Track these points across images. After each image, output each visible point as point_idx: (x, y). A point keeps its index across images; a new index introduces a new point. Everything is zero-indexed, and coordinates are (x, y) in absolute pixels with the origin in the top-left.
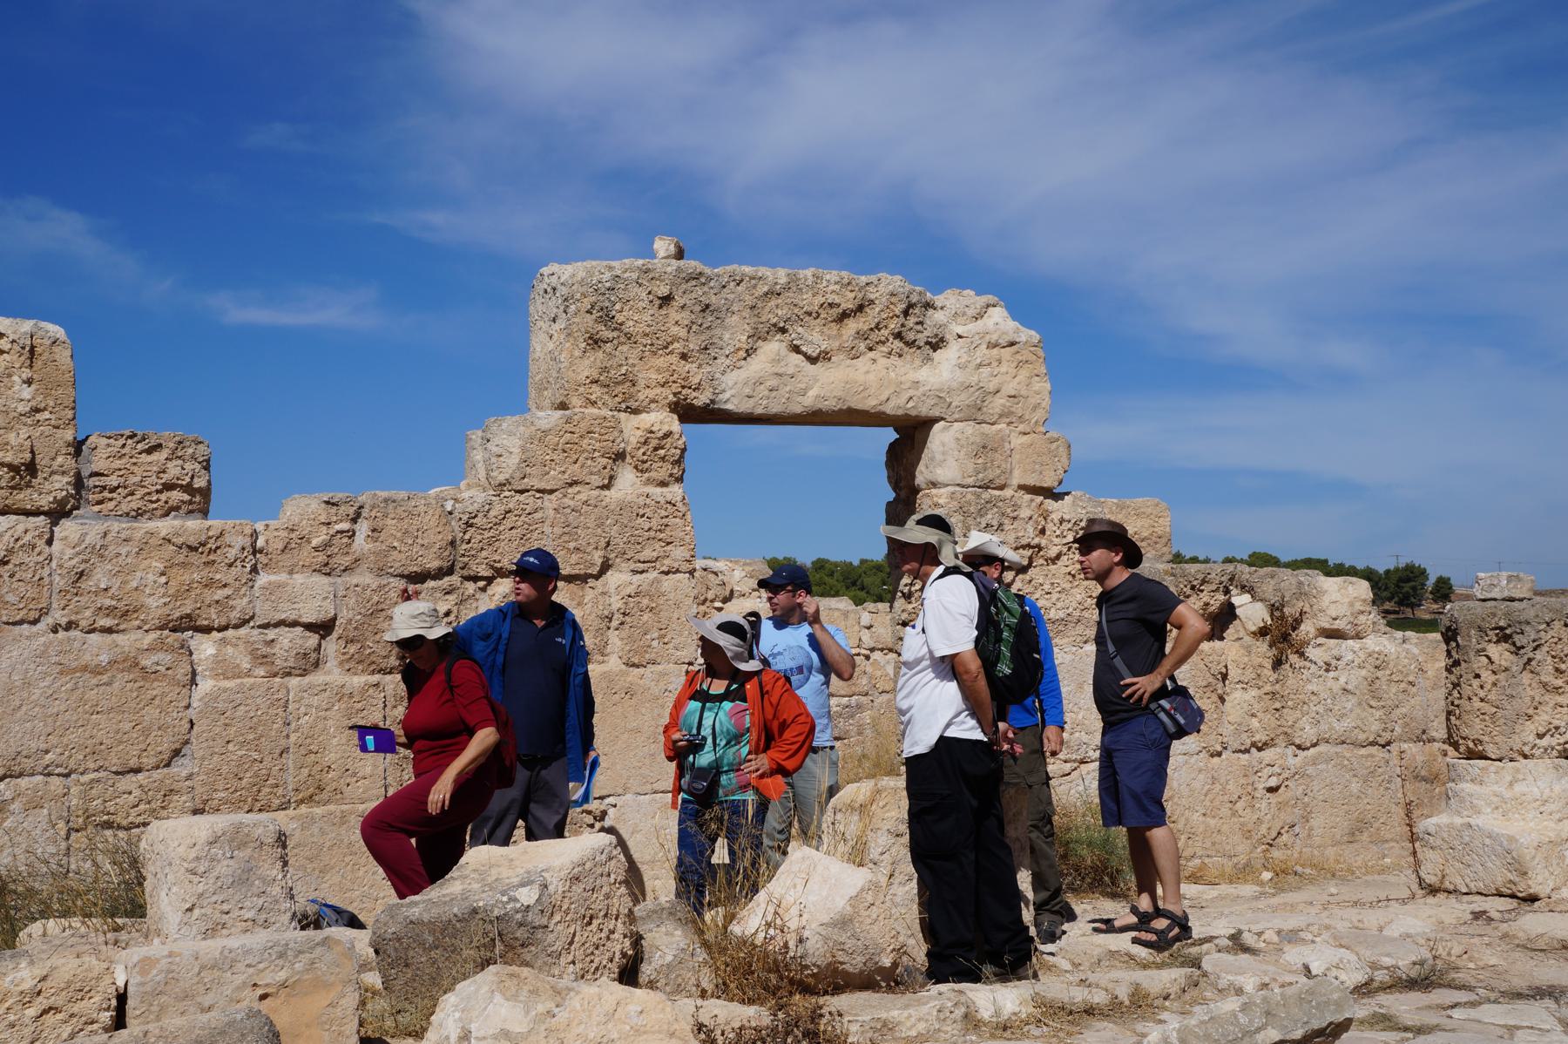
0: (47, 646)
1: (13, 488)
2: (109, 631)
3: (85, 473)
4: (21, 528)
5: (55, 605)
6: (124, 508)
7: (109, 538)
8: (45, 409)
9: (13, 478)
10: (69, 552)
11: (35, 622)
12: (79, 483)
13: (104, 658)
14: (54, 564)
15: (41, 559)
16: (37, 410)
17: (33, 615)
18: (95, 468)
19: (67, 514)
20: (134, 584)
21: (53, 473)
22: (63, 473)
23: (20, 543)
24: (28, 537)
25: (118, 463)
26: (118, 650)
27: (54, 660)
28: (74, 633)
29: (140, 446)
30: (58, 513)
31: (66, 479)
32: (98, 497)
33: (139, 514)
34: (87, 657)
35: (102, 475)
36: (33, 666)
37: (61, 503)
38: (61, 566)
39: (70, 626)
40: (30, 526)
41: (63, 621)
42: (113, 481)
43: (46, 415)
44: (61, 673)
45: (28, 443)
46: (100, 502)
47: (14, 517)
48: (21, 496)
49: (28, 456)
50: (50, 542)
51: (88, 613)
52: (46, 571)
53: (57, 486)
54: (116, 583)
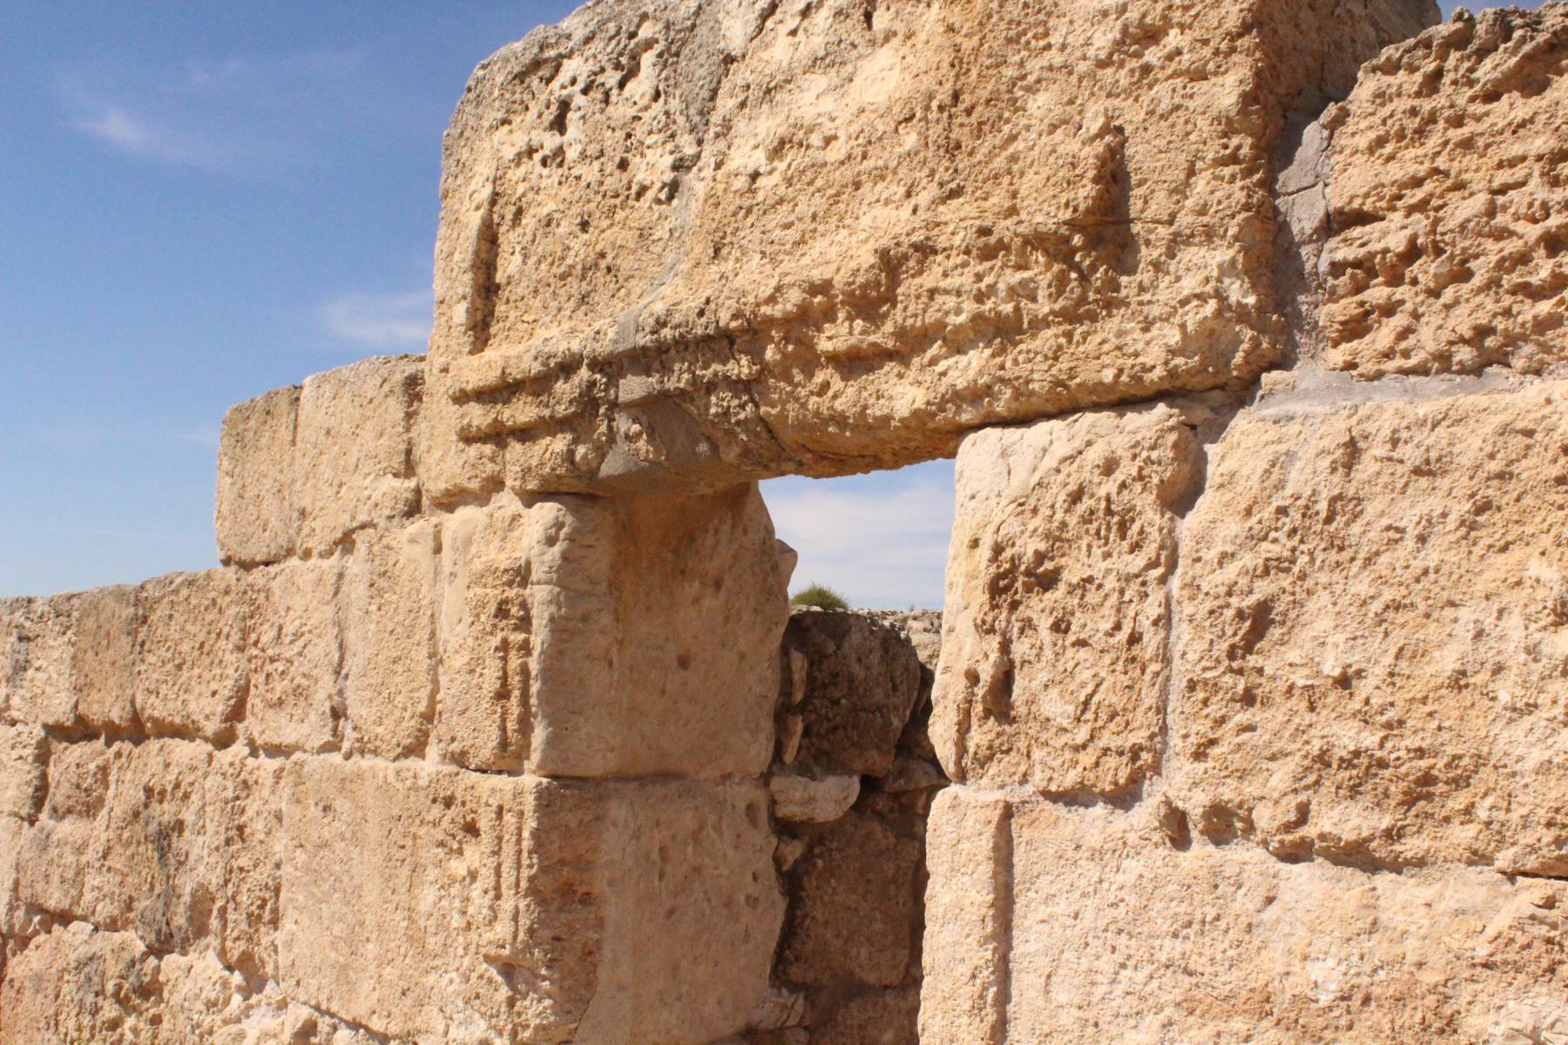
0: (1148, 888)
1: (1070, 316)
2: (1355, 856)
3: (1304, 216)
4: (1095, 455)
5: (1175, 740)
6: (1428, 339)
7: (1367, 467)
8: (1167, 23)
9: (1061, 283)
10: (1233, 527)
11: (1124, 797)
12: (1273, 259)
13: (1326, 976)
14: (1175, 582)
15: (1138, 561)
16: (1151, 36)
17: (1116, 771)
18: (1335, 197)
19: (1243, 392)
20: (1447, 661)
21: (1176, 243)
22: (1209, 234)
23: (1081, 508)
24: (1109, 487)
25: (1411, 161)
26: (1378, 947)
27: (1171, 949)
28: (1244, 855)
29: (1487, 71)
30: (1209, 393)
31: (1223, 254)
32: (1345, 308)
33: (1487, 353)
34: (1272, 961)
35: (1362, 218)
36: (1107, 964)
37: (1210, 342)
38: (1193, 586)
39: (1224, 824)
40: (1120, 444)
41: (1195, 804)
42: (1390, 235)
43: (1173, 39)
44: (1188, 1006)
45: (1099, 147)
46: (1355, 328)
47: (1090, 417)
48: (1091, 345)
49: (1085, 192)
50: (1181, 496)
51: (1280, 776)
52: (1152, 609)
53: (1189, 285)
54: (1376, 656)
